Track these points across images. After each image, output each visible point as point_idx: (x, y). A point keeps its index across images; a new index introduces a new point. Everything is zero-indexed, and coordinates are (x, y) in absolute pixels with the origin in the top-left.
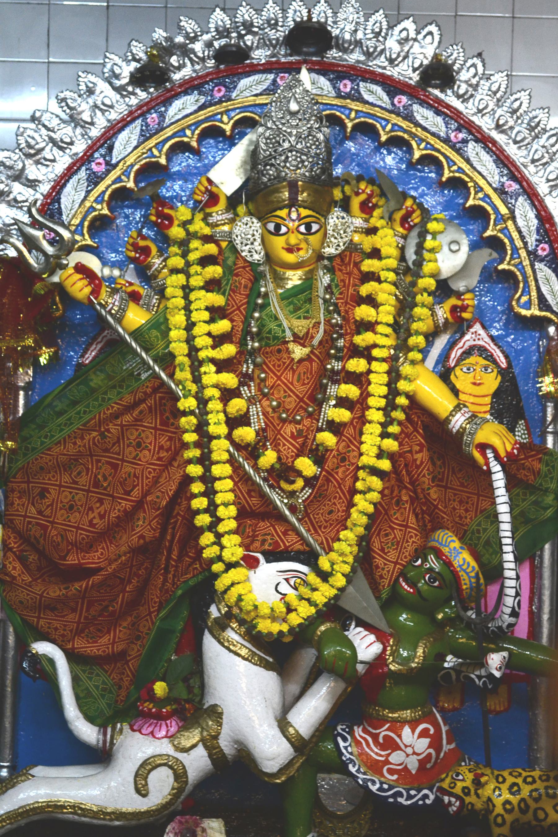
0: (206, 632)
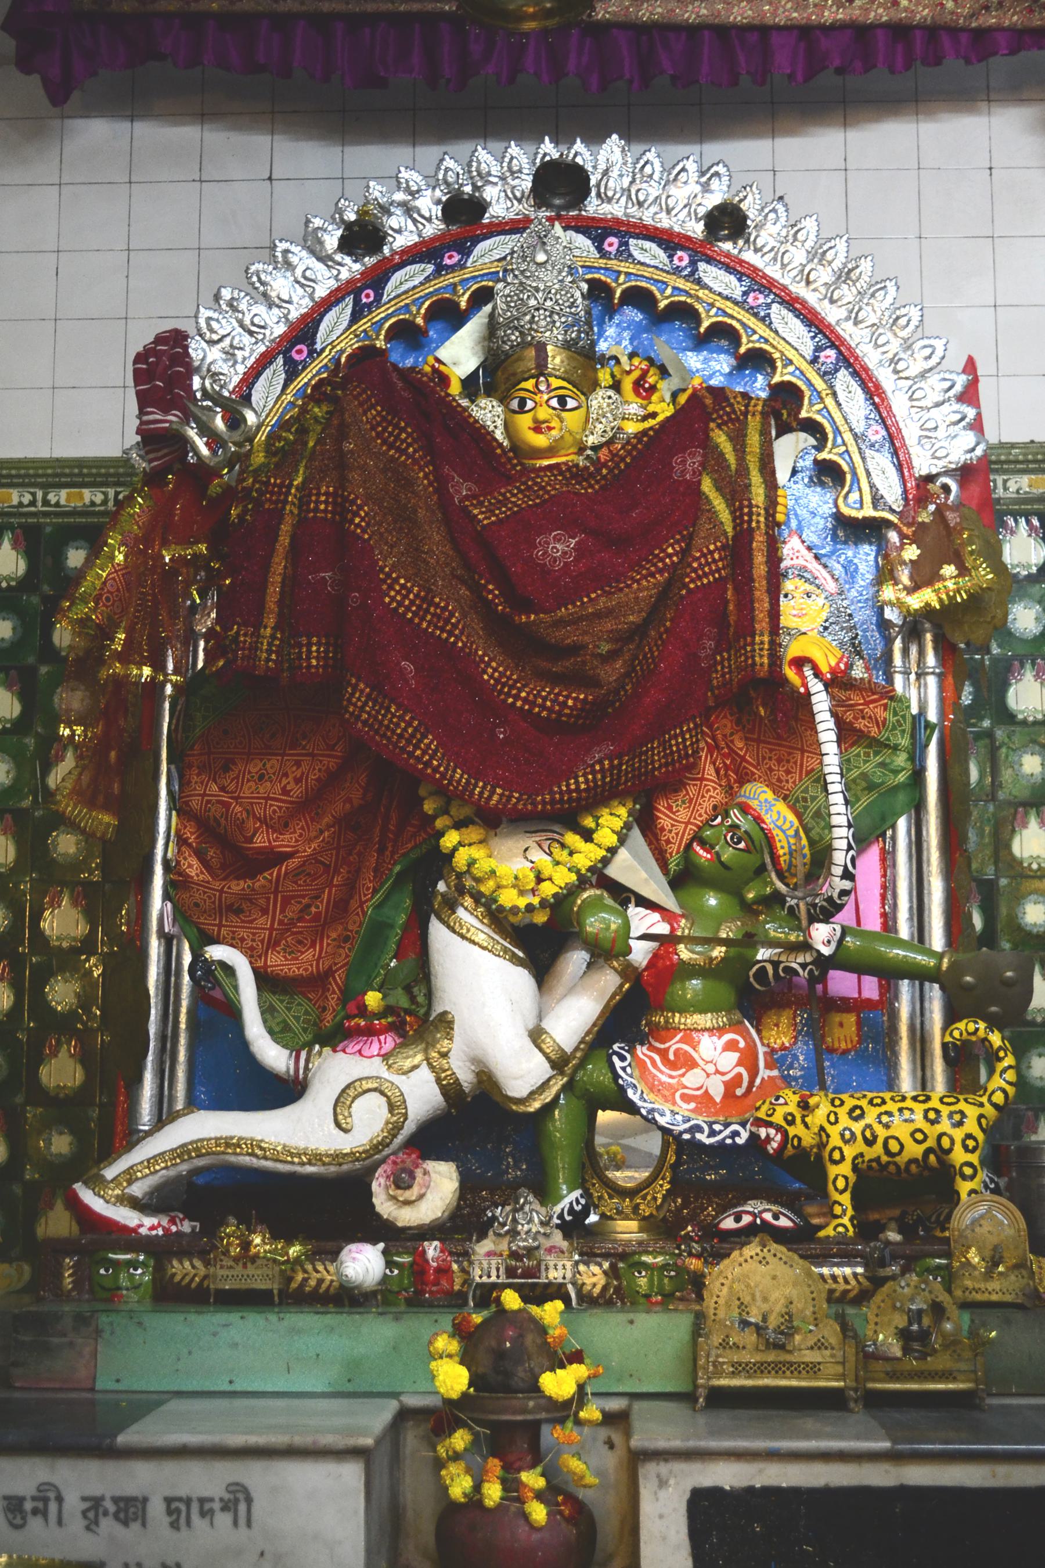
0: (433, 917)
